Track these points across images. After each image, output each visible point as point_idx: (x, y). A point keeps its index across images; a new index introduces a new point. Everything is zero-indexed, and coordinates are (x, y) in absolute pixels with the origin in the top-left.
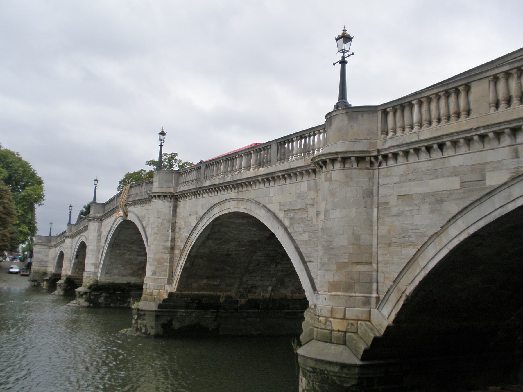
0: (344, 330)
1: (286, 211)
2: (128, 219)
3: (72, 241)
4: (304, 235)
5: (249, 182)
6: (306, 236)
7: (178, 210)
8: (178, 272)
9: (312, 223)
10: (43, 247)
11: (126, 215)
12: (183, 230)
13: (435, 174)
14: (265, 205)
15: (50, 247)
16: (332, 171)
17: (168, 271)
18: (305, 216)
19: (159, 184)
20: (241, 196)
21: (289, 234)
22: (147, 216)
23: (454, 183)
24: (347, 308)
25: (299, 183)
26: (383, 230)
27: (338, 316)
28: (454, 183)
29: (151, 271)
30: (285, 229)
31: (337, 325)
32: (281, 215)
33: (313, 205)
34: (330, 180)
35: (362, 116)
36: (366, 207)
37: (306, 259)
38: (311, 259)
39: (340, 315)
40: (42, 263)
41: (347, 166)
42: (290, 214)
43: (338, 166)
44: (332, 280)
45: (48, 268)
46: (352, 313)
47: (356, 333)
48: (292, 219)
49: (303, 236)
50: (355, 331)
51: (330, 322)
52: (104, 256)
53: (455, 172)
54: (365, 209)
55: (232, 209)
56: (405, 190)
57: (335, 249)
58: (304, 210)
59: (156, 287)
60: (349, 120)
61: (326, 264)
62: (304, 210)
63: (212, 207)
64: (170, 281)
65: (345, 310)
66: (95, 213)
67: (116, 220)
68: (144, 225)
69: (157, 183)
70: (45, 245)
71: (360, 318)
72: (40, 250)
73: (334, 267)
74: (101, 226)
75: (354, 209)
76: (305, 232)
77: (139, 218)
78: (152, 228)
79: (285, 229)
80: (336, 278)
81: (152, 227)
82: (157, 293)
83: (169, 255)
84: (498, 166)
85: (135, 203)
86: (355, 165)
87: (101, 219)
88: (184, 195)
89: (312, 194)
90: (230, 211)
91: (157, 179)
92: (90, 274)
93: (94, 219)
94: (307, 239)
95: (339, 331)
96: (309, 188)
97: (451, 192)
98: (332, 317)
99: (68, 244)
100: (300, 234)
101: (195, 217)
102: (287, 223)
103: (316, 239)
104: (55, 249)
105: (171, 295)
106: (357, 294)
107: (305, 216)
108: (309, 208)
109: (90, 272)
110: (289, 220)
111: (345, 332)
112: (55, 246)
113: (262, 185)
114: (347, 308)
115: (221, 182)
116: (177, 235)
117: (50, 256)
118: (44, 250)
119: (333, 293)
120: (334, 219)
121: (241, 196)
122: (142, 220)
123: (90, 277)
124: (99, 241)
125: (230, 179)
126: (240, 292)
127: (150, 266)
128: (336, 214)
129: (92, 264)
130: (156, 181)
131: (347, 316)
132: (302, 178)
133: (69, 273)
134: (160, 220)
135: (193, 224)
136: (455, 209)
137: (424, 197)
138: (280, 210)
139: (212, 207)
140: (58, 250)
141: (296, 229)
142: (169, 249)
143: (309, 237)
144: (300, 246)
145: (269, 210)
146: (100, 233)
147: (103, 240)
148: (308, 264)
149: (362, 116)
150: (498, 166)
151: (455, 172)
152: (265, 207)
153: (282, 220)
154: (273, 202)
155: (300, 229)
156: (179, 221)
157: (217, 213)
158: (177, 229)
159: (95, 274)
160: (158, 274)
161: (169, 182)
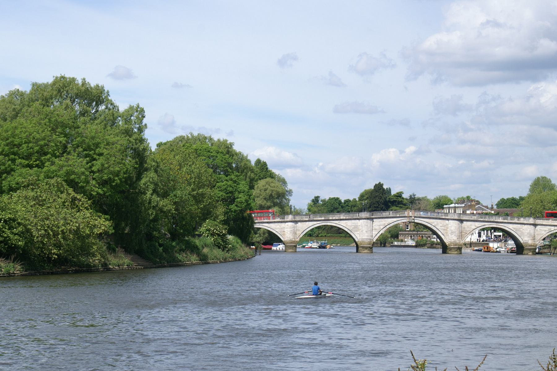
1: (514, 229)
13: (545, 228)
23: (548, 229)
26: (537, 233)
28: (548, 229)
31: (532, 244)
32: (513, 229)
46: (534, 243)
48: (516, 230)
53: (548, 228)
56: (541, 229)
58: (520, 229)
84: (552, 228)
89: (521, 227)
97: (547, 230)
102: (514, 230)
136: (547, 232)
137: (543, 230)
139: (485, 225)
150: (552, 228)
151: (548, 228)
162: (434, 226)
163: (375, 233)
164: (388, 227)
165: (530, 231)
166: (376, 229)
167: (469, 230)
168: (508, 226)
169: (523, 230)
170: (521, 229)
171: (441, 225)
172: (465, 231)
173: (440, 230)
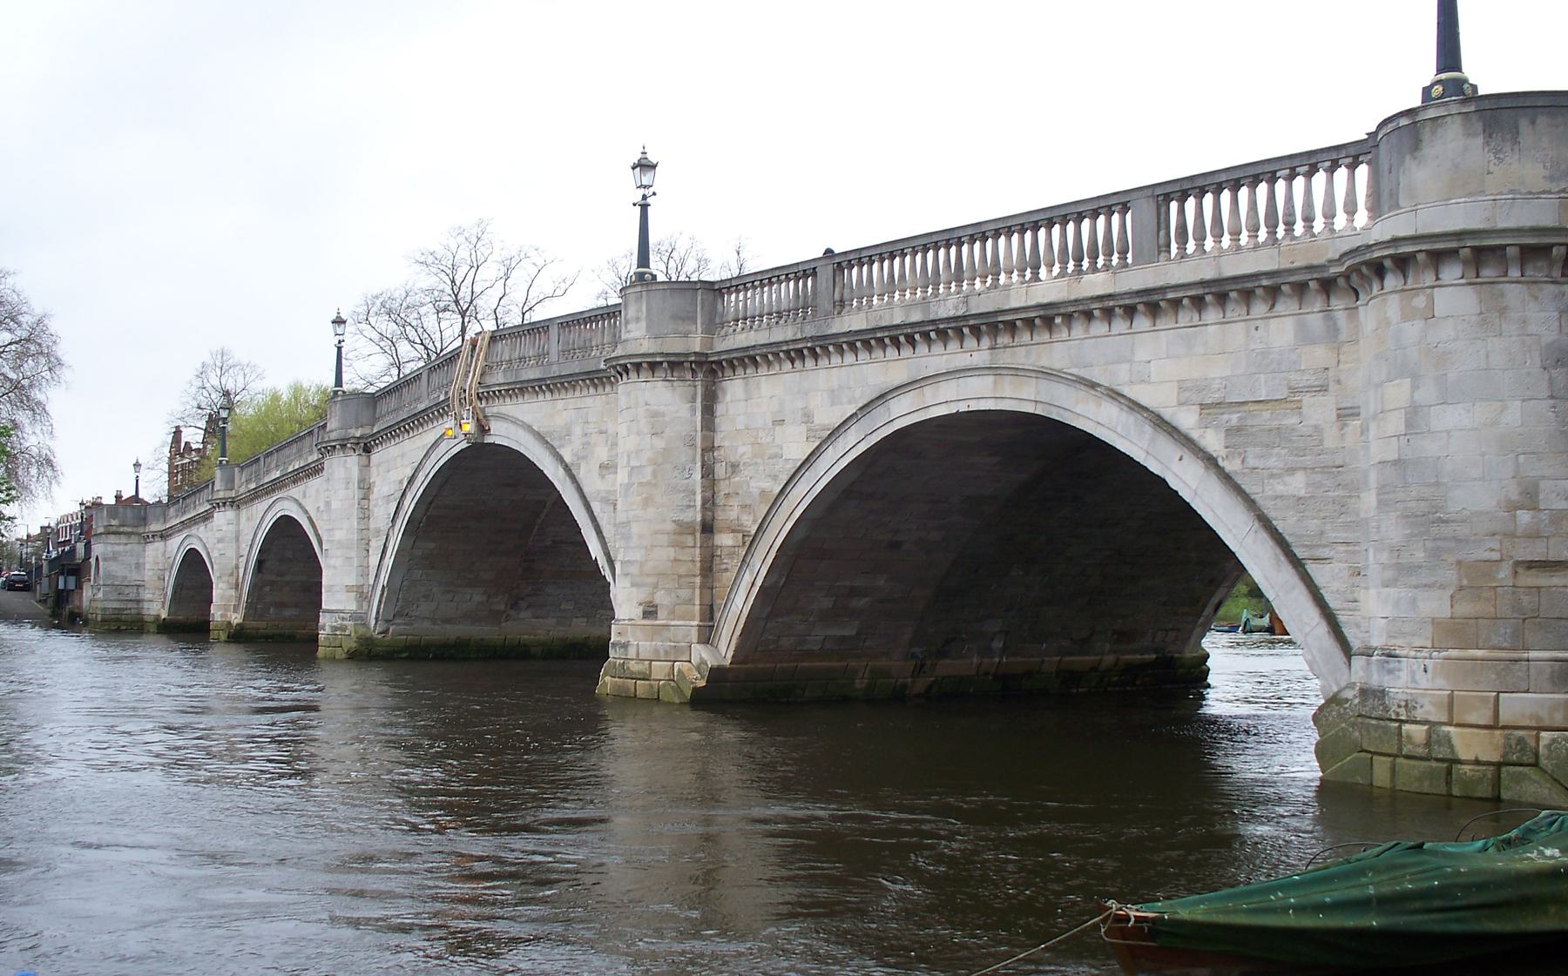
0: (1496, 758)
2: (488, 440)
3: (238, 517)
4: (1288, 479)
5: (1047, 318)
6: (1297, 484)
7: (720, 409)
8: (739, 605)
9: (1321, 442)
10: (124, 539)
11: (483, 429)
12: (746, 473)
14: (1118, 388)
15: (147, 539)
16: (1433, 287)
17: (697, 602)
18: (1292, 420)
19: (648, 328)
20: (1005, 359)
21: (1226, 478)
22: (577, 430)
24: (1501, 694)
25: (1258, 323)
27: (1473, 718)
29: (641, 604)
30: (1210, 461)
32: (1187, 420)
33: (1323, 389)
34: (1429, 315)
35: (1533, 122)
36: (1552, 397)
37: (1300, 553)
38: (1321, 553)
39: (1482, 716)
40: (127, 591)
41: (1488, 273)
42: (1225, 417)
43: (1451, 273)
44: (1444, 611)
45: (146, 605)
47: (1536, 765)
49: (1285, 484)
50: (1532, 761)
51: (1448, 739)
52: (389, 561)
54: (1552, 402)
55: (969, 402)
57: (1453, 521)
58: (1290, 401)
59: (662, 653)
60: (1489, 132)
61: (1420, 567)
62: (1290, 401)
63: (882, 397)
64: (707, 635)
65: (1497, 699)
66: (344, 427)
67: (436, 444)
68: (568, 459)
69: (643, 324)
70: (129, 534)
71: (1547, 723)
72: (117, 548)
73: (1450, 576)
74: (368, 465)
75: (1519, 403)
76: (1292, 470)
77: (540, 437)
78: (633, 468)
79: (1210, 461)
80: (1465, 608)
81: (633, 463)
82: (667, 670)
83: (698, 551)
85: (520, 389)
86: (1514, 273)
87: (366, 447)
88: (749, 359)
90: (963, 407)
91: (639, 310)
92: (343, 619)
93: (343, 446)
94: (1302, 493)
95: (1477, 762)
96: (1305, 337)
98: (1450, 724)
99: (224, 528)
100: (1272, 476)
101: (804, 428)
102: (1213, 442)
103: (1340, 492)
104: (163, 543)
105: (716, 674)
106: (1533, 654)
107: (1292, 420)
108: (1307, 399)
109: (342, 611)
110: (1222, 435)
111: (1499, 765)
112: (164, 536)
113: (1099, 327)
114: (1455, 692)
115: (916, 317)
116: (723, 488)
117: (147, 567)
118: (129, 547)
119: (1454, 653)
120: (1448, 432)
121: (1005, 359)
122: (555, 444)
123: (343, 628)
124: (365, 515)
125: (956, 308)
126: (914, 656)
127: (634, 589)
128: (1451, 418)
129: (349, 589)
130: (638, 320)
131: (1505, 717)
132: (1273, 306)
133: (236, 618)
134: (659, 443)
135: (798, 450)
138: (1181, 404)
139: (882, 397)
140: (175, 548)
141: (1251, 462)
142: (698, 535)
143: (1308, 485)
144: (1271, 514)
145: (1135, 406)
146: (366, 488)
147: (381, 513)
148: (1311, 568)
149: (1533, 122)
152: (1115, 395)
153: (1195, 435)
154: (1153, 379)
155: (1272, 462)
156: (726, 444)
157: (903, 413)
158: (720, 471)
159: (359, 618)
160: (662, 613)
161: (683, 320)
162: (567, 468)
163: (374, 560)
164: (409, 505)
165: (1414, 415)
166: (378, 531)
167: (763, 493)
168: (1120, 378)
169: (1346, 414)
170: (1320, 411)
171: (602, 454)
172: (733, 514)
173: (596, 506)
